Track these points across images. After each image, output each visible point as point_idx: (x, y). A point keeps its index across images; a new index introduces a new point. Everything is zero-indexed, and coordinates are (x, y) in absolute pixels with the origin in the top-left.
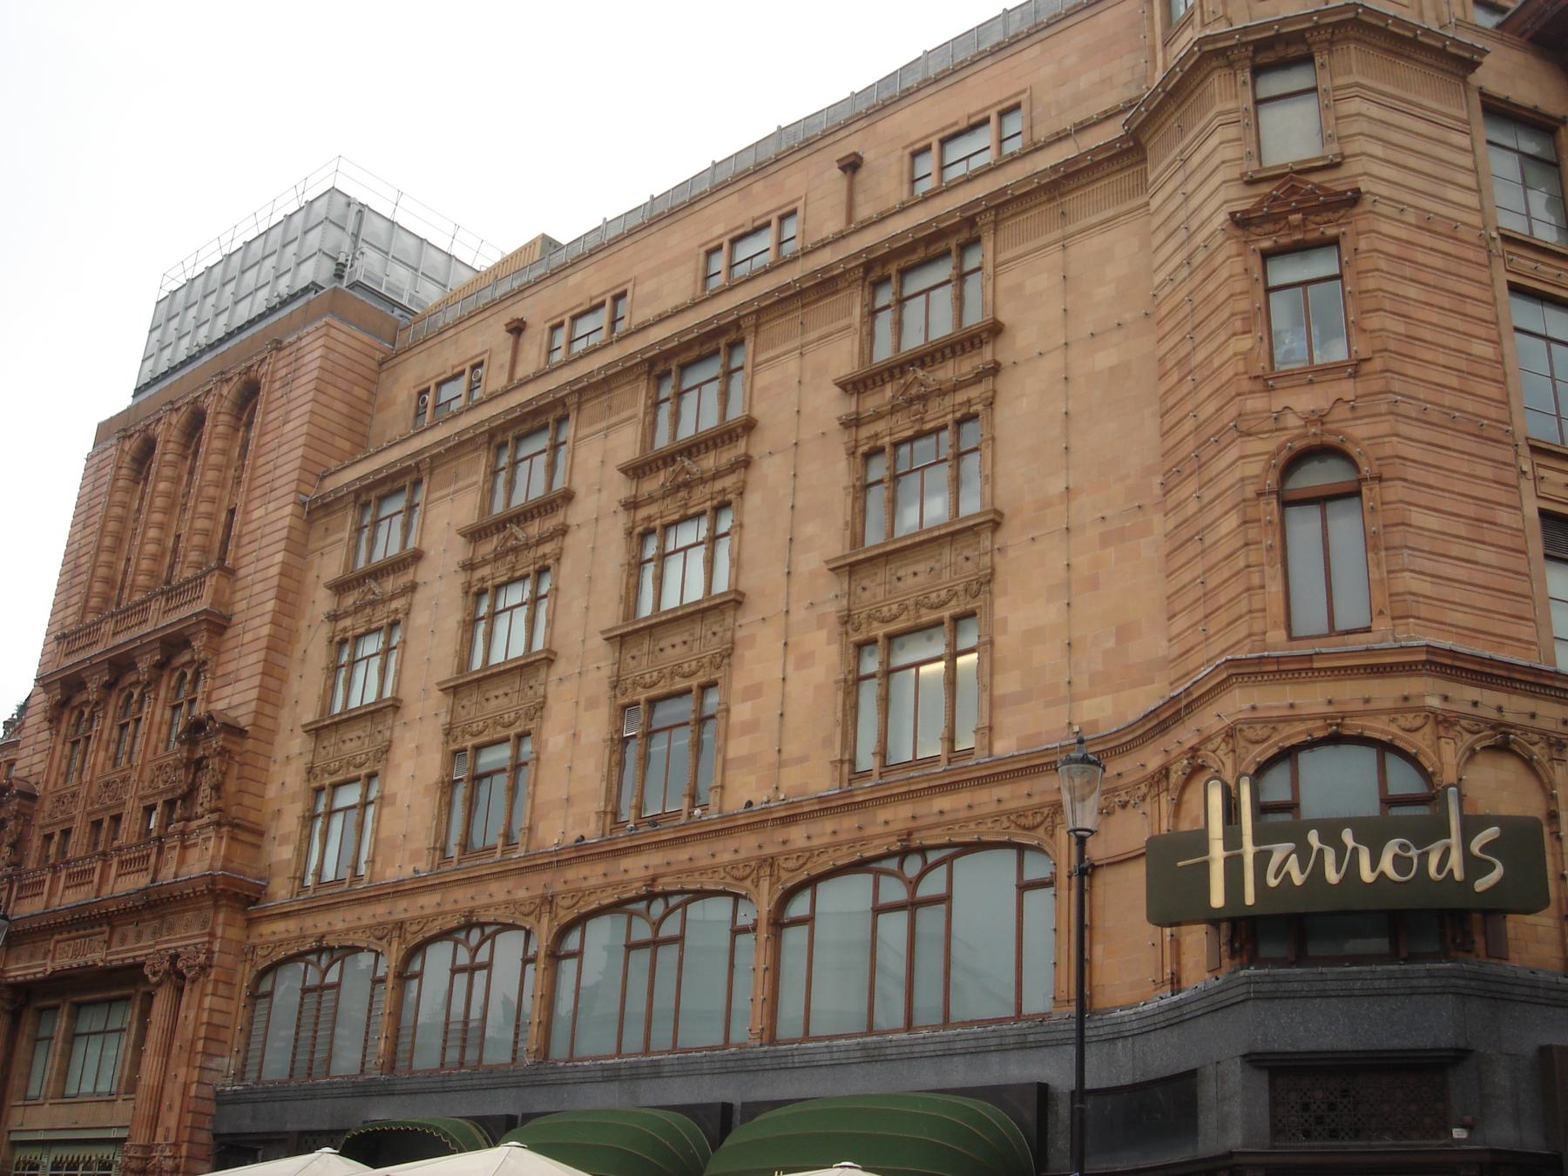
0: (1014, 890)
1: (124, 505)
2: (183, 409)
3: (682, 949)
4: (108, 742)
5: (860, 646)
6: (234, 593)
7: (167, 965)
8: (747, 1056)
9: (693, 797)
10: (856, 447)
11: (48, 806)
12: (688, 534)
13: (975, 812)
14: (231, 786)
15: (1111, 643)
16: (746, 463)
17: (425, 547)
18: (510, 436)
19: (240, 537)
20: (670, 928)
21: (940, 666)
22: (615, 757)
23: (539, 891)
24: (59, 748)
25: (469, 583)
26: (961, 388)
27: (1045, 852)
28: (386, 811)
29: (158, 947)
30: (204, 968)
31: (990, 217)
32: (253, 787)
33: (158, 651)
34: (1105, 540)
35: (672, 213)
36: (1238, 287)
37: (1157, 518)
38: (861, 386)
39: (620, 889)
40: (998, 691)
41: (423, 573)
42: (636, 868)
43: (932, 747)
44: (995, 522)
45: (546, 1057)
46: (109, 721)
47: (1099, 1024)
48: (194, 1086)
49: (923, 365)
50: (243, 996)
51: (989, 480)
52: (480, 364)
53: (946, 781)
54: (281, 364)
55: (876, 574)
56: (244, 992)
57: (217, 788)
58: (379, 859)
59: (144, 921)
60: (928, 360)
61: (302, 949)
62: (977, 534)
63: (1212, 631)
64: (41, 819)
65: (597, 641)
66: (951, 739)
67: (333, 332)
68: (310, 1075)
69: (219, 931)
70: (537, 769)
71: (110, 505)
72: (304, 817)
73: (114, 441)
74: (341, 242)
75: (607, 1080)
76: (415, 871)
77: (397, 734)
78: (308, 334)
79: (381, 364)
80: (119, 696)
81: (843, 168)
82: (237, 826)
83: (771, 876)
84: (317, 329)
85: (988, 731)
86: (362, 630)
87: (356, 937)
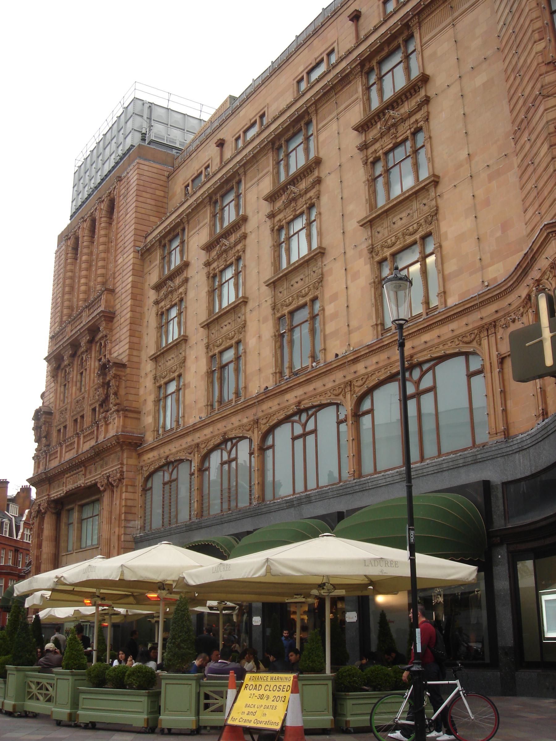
0: (466, 377)
1: (71, 271)
2: (88, 220)
3: (316, 436)
4: (76, 382)
5: (381, 263)
6: (115, 300)
7: (106, 481)
8: (348, 486)
9: (313, 357)
10: (367, 160)
11: (57, 416)
12: (299, 224)
13: (442, 339)
14: (122, 392)
15: (499, 234)
16: (319, 181)
18: (218, 196)
19: (114, 273)
20: (310, 426)
21: (418, 266)
22: (278, 344)
23: (252, 418)
24: (59, 388)
25: (209, 272)
26: (413, 115)
27: (478, 354)
28: (187, 391)
29: (103, 473)
30: (120, 480)
31: (416, 20)
32: (133, 391)
33: (88, 335)
34: (491, 178)
35: (280, 67)
36: (534, 15)
37: (515, 159)
38: (365, 127)
39: (286, 410)
40: (447, 272)
42: (291, 398)
43: (418, 309)
44: (435, 181)
45: (263, 500)
46: (75, 372)
47: (511, 444)
48: (123, 536)
49: (393, 109)
50: (140, 491)
51: (431, 160)
53: (426, 325)
55: (383, 223)
56: (141, 489)
57: (116, 394)
58: (186, 416)
59: (97, 462)
60: (395, 105)
61: (160, 464)
62: (428, 190)
63: (543, 213)
65: (264, 289)
66: (427, 302)
67: (142, 166)
68: (170, 524)
69: (125, 462)
70: (245, 357)
71: (65, 272)
72: (155, 401)
73: (64, 242)
74: (141, 123)
75: (288, 507)
76: (200, 418)
77: (187, 353)
78: (131, 170)
79: (168, 177)
80: (78, 359)
81: (351, 20)
82: (127, 410)
83: (351, 391)
84: (134, 166)
85: (444, 294)
86: (169, 306)
87: (181, 454)
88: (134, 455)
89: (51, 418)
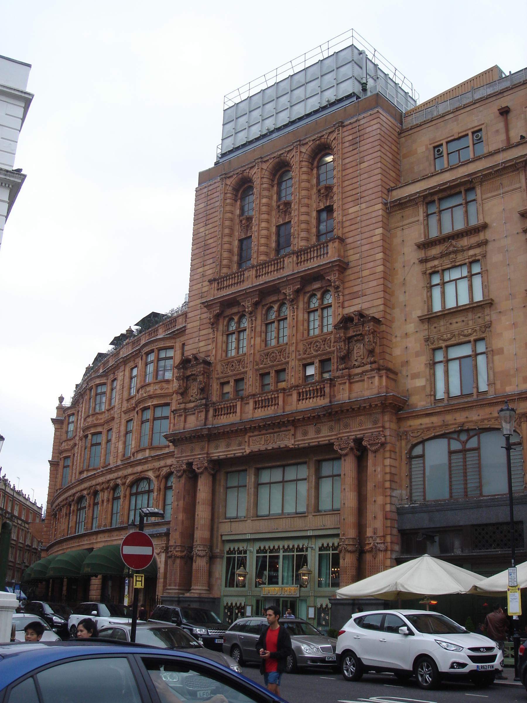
6: (345, 251)
11: (219, 368)
14: (378, 350)
17: (487, 221)
29: (339, 436)
30: (383, 445)
41: (488, 235)
50: (404, 457)
52: (480, 130)
54: (346, 134)
59: (322, 423)
64: (215, 375)
69: (387, 425)
71: (225, 212)
78: (364, 118)
84: (371, 115)
88: (394, 418)
89: (209, 369)
